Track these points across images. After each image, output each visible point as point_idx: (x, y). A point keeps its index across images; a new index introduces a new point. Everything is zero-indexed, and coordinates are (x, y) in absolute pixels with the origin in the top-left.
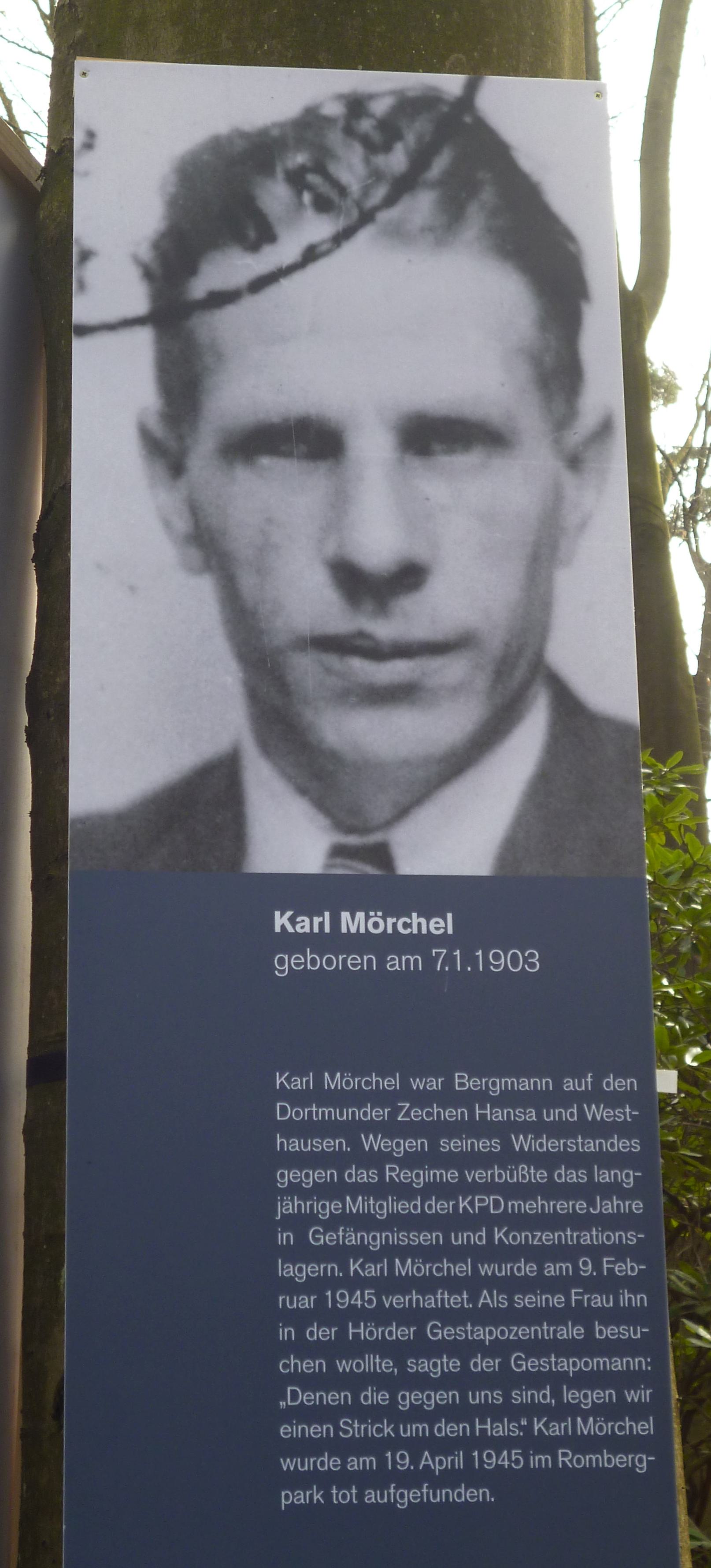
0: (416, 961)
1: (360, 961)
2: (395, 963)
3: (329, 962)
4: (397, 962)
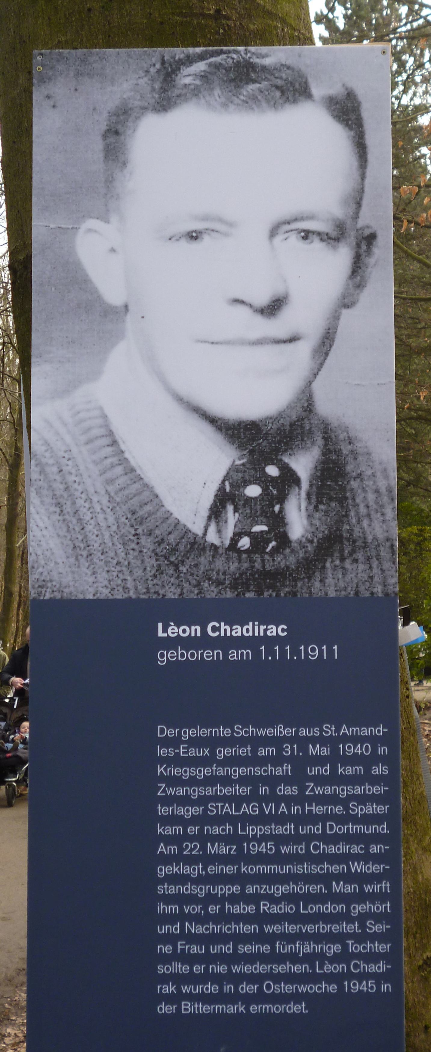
0: (248, 653)
2: (234, 655)
4: (235, 654)
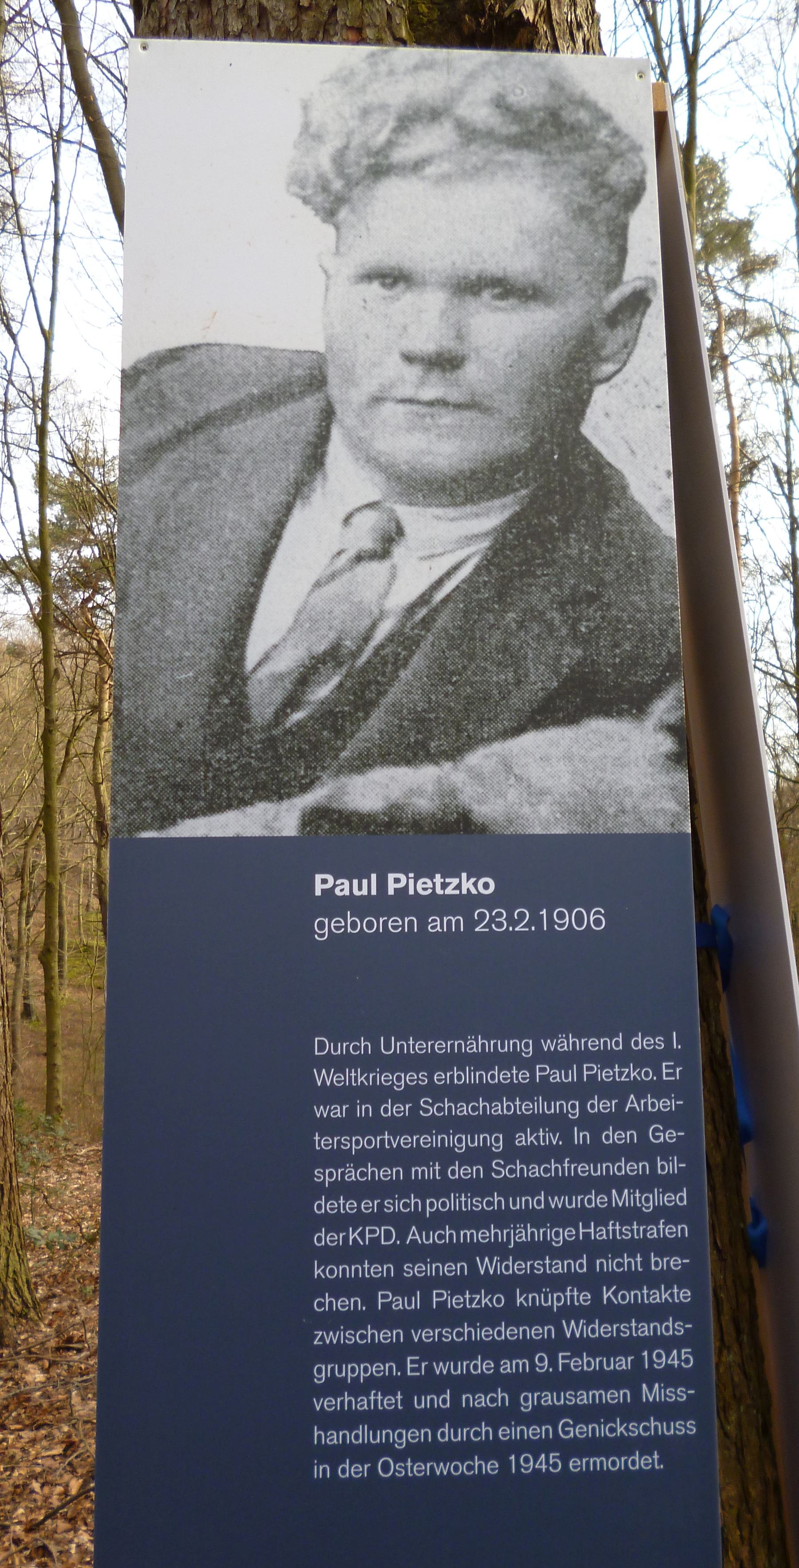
0: (458, 921)
2: (436, 925)
3: (370, 925)
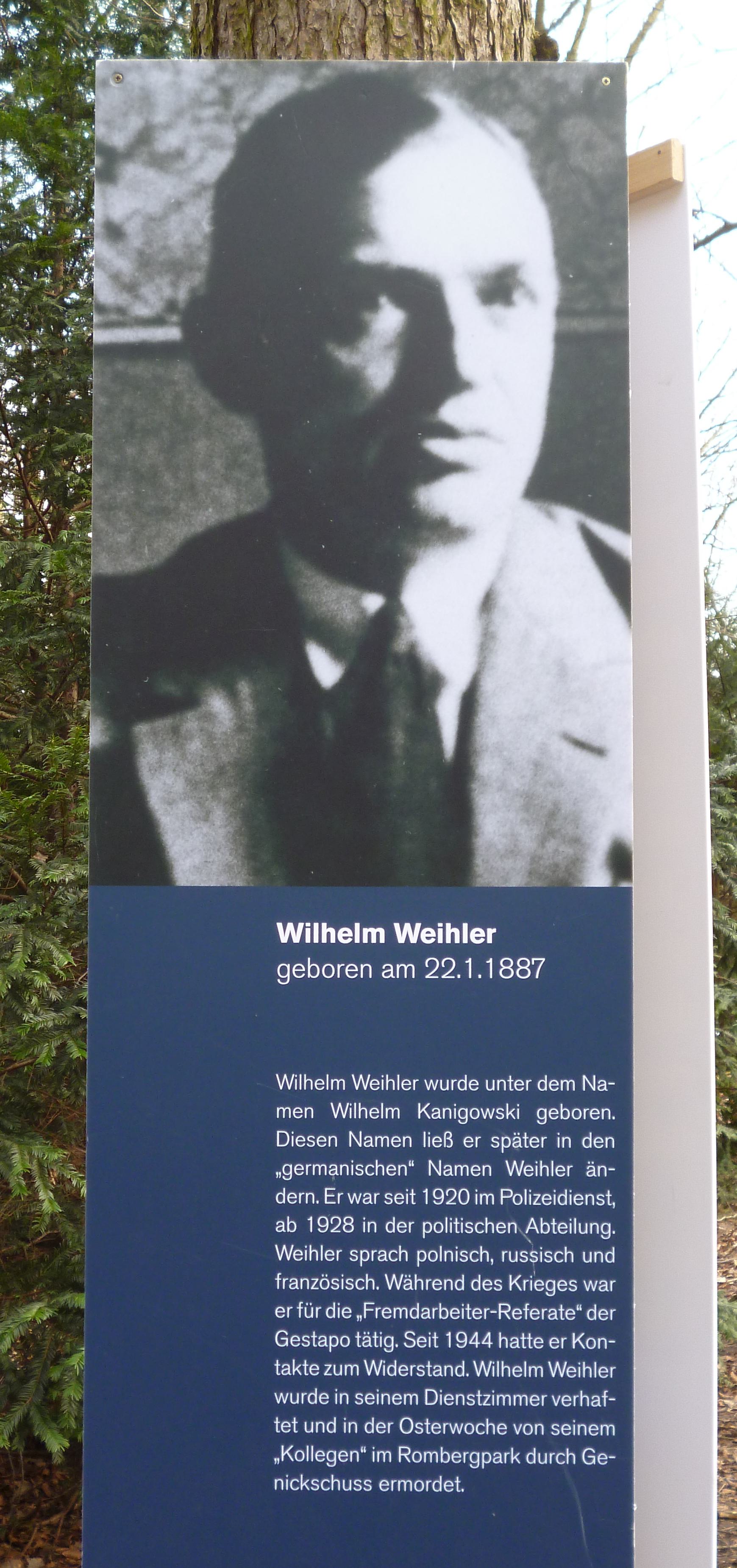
0: (410, 969)
1: (357, 970)
2: (389, 972)
4: (392, 970)
